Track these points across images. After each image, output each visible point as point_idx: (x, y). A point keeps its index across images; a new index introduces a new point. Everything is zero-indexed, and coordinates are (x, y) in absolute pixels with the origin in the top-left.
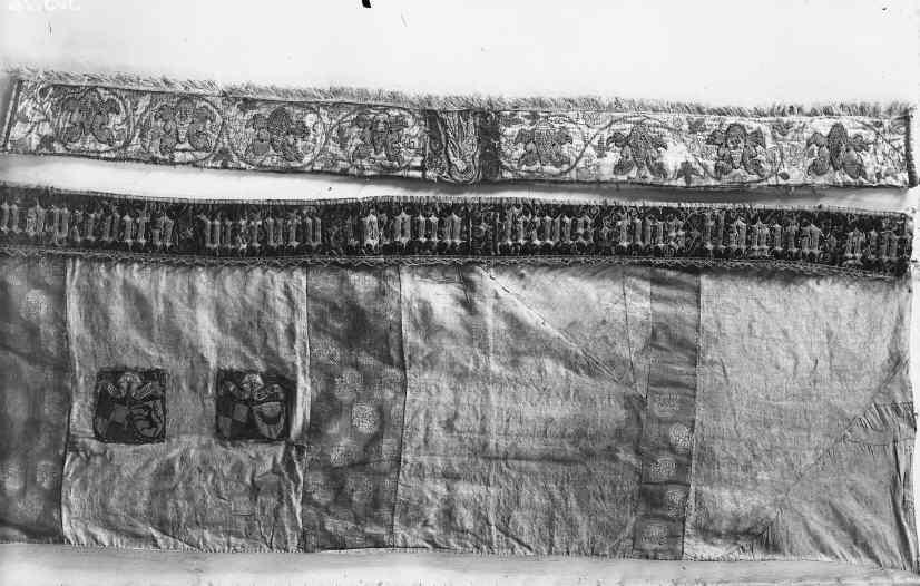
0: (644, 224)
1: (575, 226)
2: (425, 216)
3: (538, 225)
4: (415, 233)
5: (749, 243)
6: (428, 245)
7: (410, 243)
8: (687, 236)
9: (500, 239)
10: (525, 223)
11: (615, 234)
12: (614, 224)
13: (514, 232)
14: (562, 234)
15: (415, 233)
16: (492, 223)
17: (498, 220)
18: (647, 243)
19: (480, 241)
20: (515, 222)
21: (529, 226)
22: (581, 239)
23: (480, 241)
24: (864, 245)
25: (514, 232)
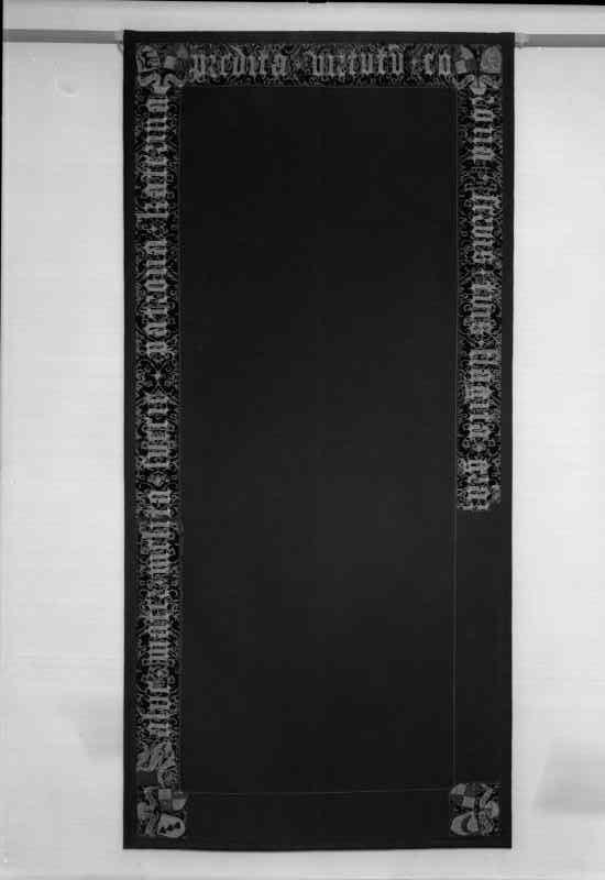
0: (489, 303)
1: (486, 249)
2: (493, 132)
3: (487, 221)
4: (480, 124)
5: (476, 384)
6: (471, 134)
7: (473, 121)
8: (480, 336)
9: (476, 191)
10: (487, 211)
11: (480, 279)
12: (488, 279)
13: (481, 202)
14: (481, 239)
15: (480, 124)
16: (488, 184)
17: (490, 190)
18: (475, 305)
19: (475, 175)
20: (489, 203)
21: (485, 214)
22: (476, 254)
23: (475, 175)
24: (477, 473)
25: (481, 202)
